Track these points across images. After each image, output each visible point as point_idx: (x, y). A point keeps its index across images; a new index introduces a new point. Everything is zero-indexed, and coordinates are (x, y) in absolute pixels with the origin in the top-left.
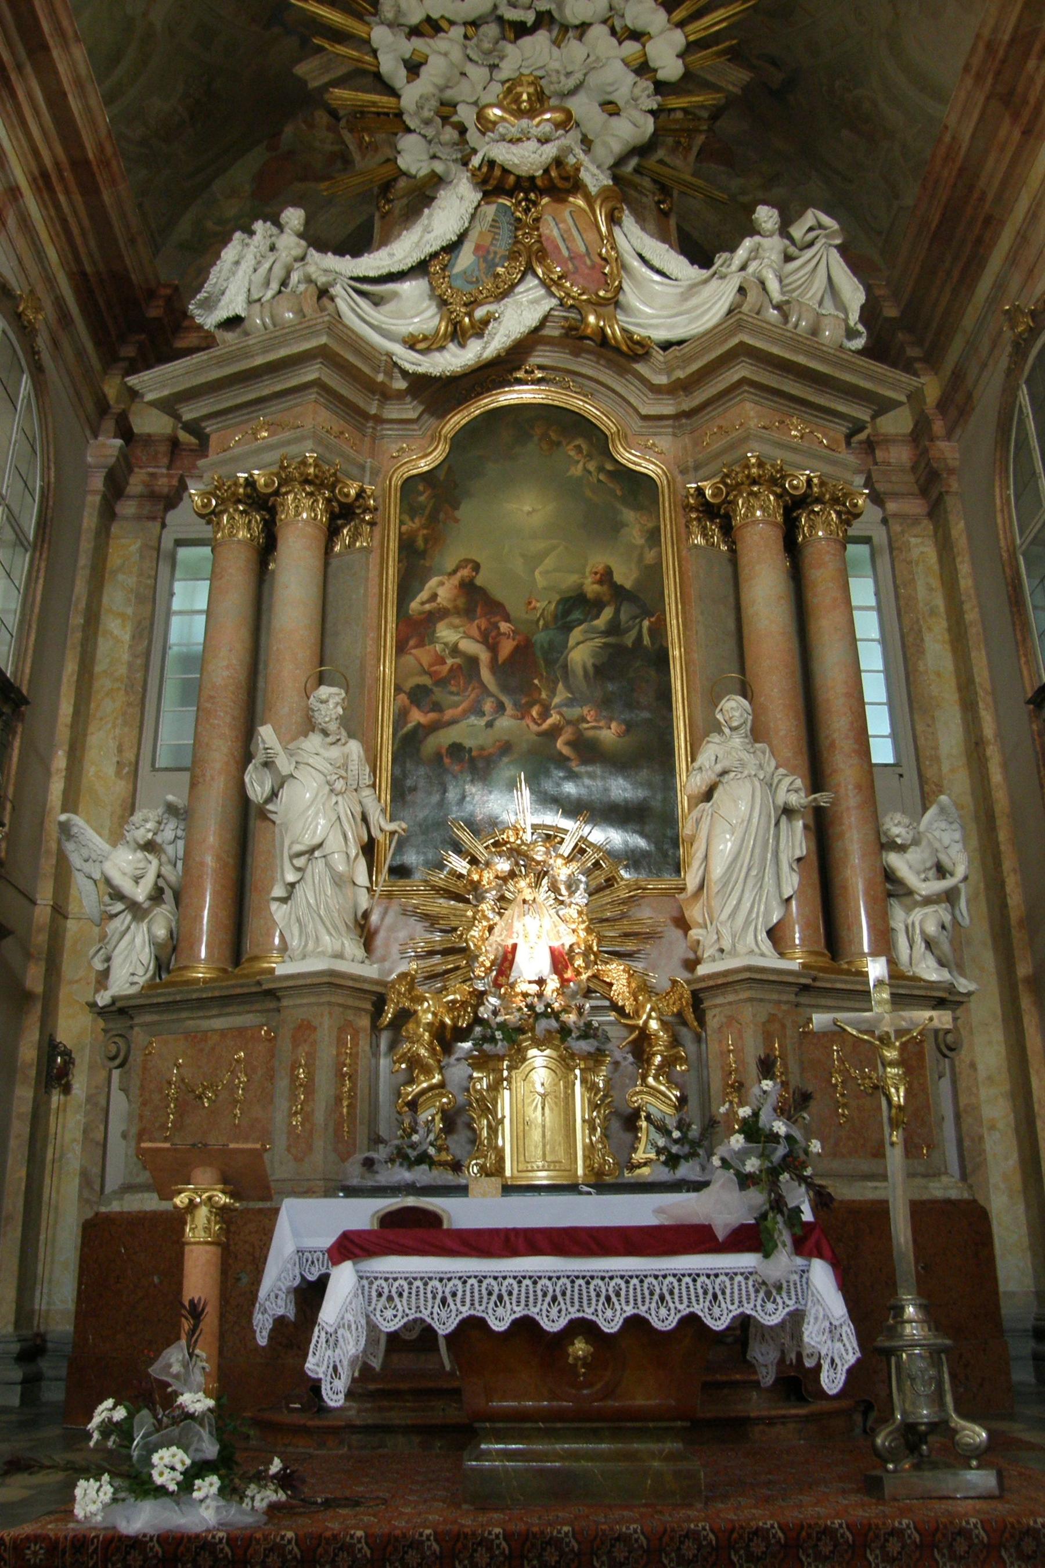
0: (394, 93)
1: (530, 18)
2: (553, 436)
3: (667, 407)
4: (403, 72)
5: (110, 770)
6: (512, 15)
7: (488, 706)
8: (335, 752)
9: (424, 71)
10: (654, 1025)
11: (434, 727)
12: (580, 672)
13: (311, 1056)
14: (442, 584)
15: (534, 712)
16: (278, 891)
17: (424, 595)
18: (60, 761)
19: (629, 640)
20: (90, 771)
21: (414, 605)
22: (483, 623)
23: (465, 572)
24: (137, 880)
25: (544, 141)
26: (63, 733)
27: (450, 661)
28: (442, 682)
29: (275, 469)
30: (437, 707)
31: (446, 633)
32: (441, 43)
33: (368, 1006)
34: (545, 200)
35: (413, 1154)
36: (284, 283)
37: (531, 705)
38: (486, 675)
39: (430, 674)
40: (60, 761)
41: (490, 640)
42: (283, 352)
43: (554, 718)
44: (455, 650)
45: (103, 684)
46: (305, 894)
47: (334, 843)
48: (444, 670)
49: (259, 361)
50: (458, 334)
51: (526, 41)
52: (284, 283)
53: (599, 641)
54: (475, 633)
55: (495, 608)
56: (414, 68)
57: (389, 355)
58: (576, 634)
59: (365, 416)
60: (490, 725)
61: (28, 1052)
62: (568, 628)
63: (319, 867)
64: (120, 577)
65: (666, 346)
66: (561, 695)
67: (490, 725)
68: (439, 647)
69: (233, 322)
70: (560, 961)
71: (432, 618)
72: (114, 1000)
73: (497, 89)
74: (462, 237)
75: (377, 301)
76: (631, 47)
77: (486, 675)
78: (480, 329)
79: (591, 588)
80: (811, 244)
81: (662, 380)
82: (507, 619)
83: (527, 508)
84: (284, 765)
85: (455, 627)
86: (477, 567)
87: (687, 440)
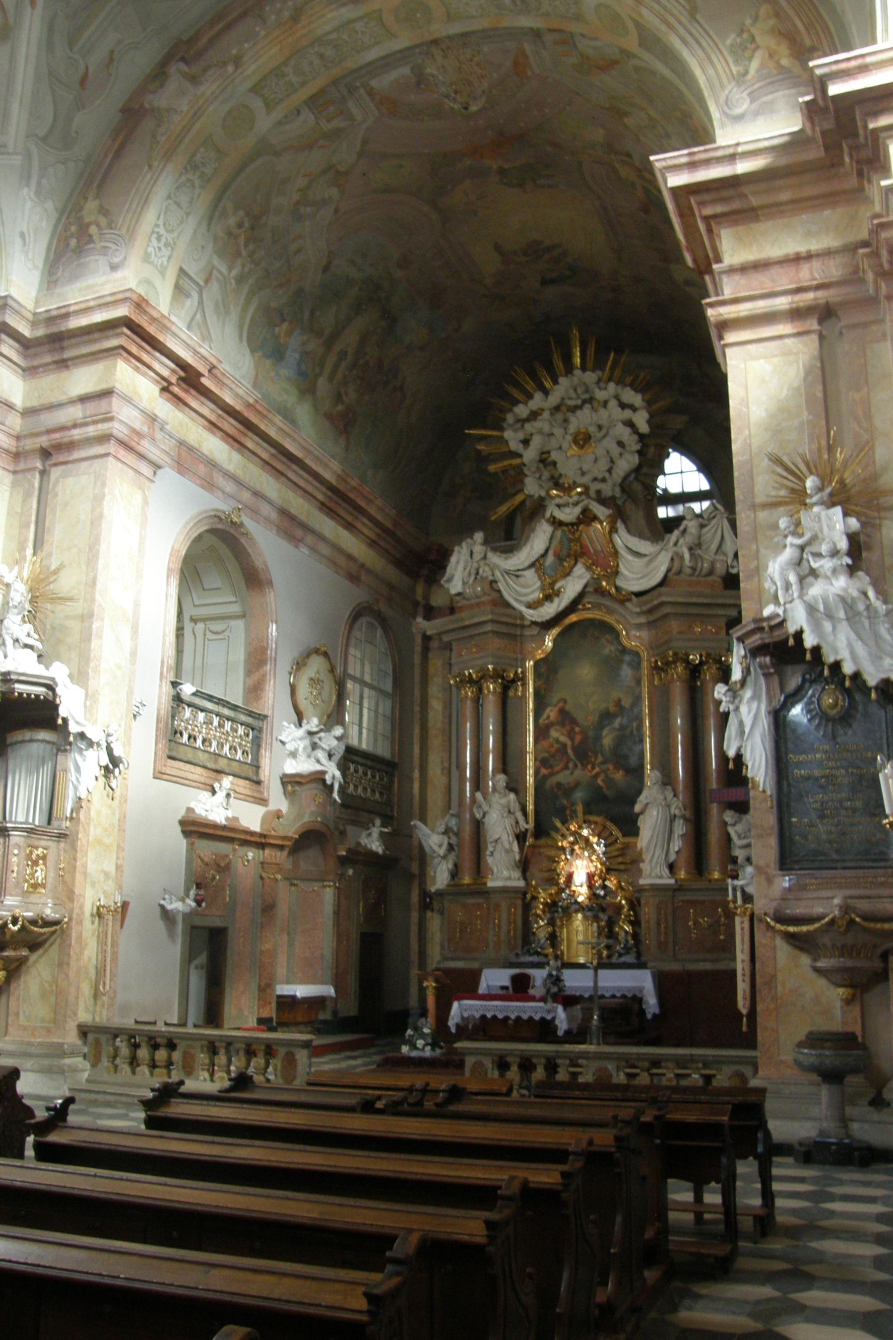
0: (520, 456)
1: (579, 402)
2: (596, 634)
3: (642, 620)
4: (521, 446)
5: (439, 772)
6: (571, 403)
7: (571, 765)
8: (503, 801)
9: (532, 443)
10: (623, 902)
11: (551, 775)
12: (607, 748)
13: (500, 917)
14: (551, 710)
15: (589, 767)
16: (488, 853)
17: (545, 716)
18: (416, 774)
19: (627, 732)
20: (431, 773)
21: (541, 721)
22: (568, 728)
23: (561, 704)
24: (440, 846)
25: (576, 504)
26: (416, 761)
27: (555, 746)
28: (553, 756)
29: (478, 668)
30: (551, 767)
31: (554, 733)
32: (537, 424)
33: (520, 896)
34: (581, 527)
35: (532, 951)
36: (477, 573)
37: (587, 764)
38: (570, 751)
39: (548, 752)
40: (416, 774)
41: (571, 735)
42: (476, 620)
43: (597, 769)
44: (557, 741)
45: (432, 732)
46: (497, 855)
47: (504, 837)
48: (553, 750)
49: (467, 623)
50: (548, 598)
51: (579, 413)
52: (477, 573)
53: (615, 734)
54: (565, 732)
55: (574, 722)
56: (526, 442)
57: (520, 612)
58: (605, 732)
59: (515, 636)
60: (572, 773)
61: (415, 897)
62: (602, 728)
63: (499, 846)
64: (435, 679)
65: (639, 594)
66: (600, 759)
67: (572, 773)
68: (551, 740)
69: (459, 594)
70: (590, 877)
71: (548, 727)
72: (437, 890)
73: (569, 438)
74: (547, 551)
75: (517, 576)
76: (627, 414)
77: (570, 751)
78: (558, 593)
79: (612, 709)
80: (714, 517)
81: (638, 610)
82: (578, 725)
83: (585, 672)
84: (485, 808)
85: (556, 730)
86: (565, 702)
87: (653, 632)
